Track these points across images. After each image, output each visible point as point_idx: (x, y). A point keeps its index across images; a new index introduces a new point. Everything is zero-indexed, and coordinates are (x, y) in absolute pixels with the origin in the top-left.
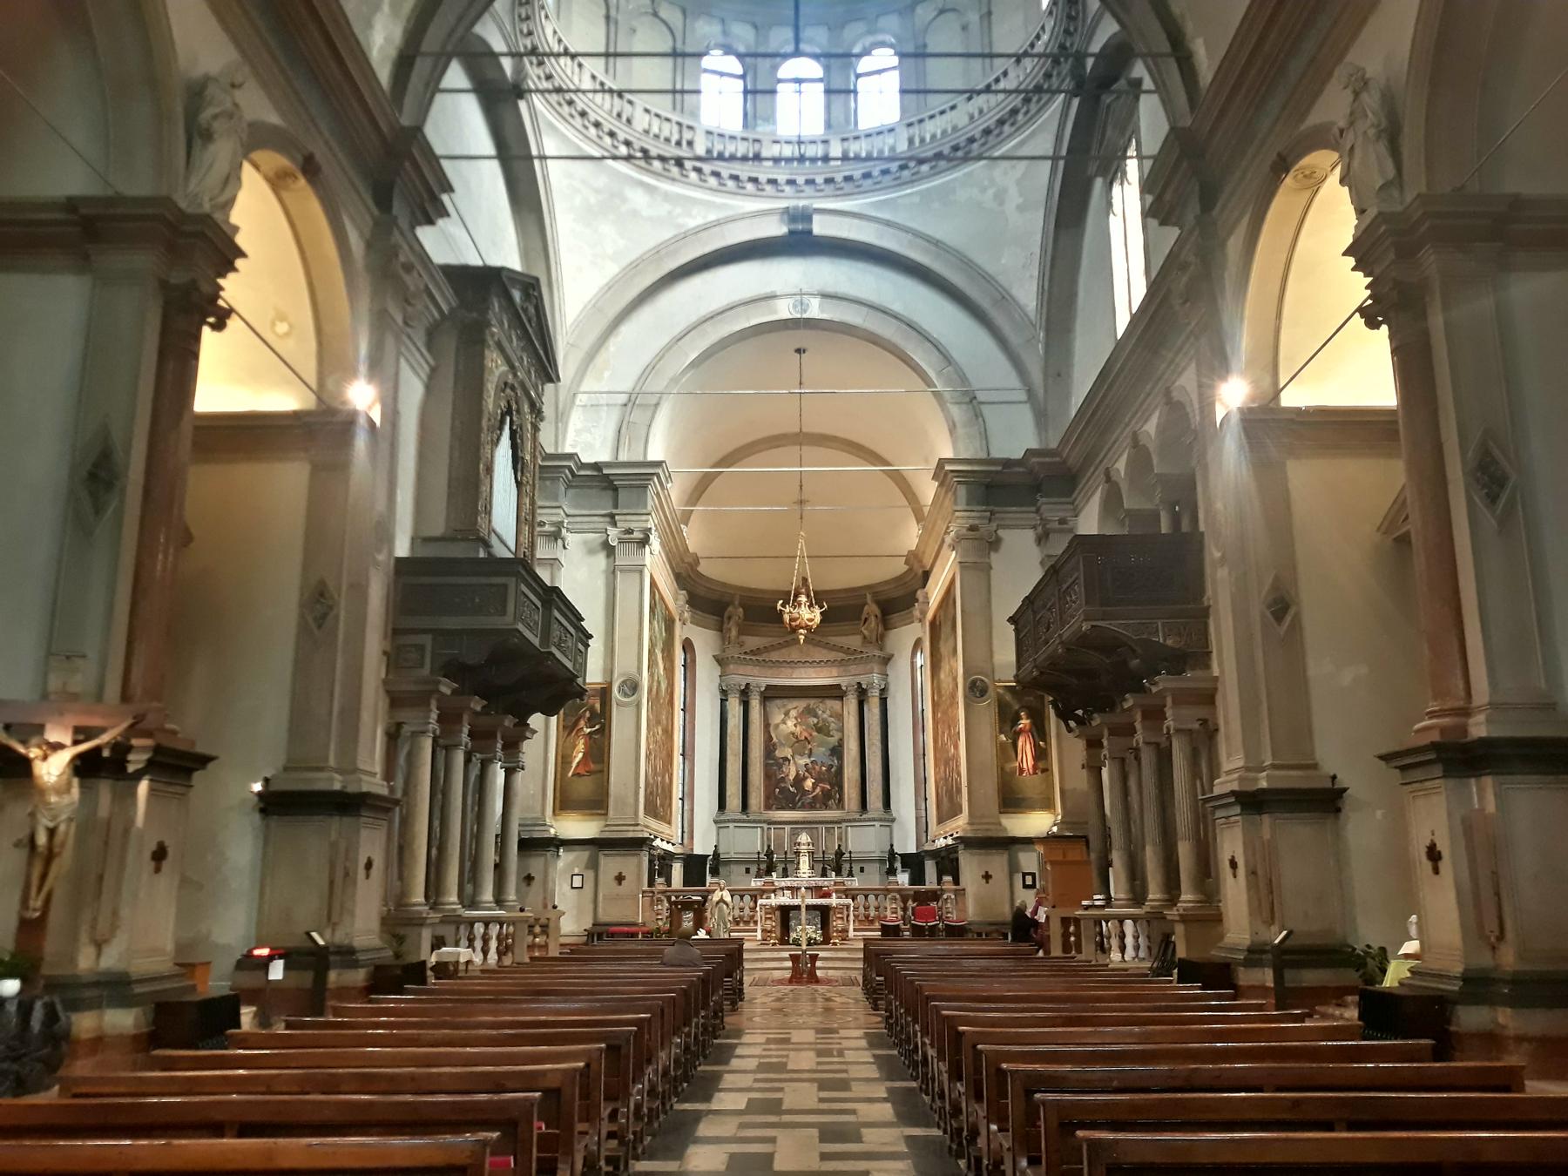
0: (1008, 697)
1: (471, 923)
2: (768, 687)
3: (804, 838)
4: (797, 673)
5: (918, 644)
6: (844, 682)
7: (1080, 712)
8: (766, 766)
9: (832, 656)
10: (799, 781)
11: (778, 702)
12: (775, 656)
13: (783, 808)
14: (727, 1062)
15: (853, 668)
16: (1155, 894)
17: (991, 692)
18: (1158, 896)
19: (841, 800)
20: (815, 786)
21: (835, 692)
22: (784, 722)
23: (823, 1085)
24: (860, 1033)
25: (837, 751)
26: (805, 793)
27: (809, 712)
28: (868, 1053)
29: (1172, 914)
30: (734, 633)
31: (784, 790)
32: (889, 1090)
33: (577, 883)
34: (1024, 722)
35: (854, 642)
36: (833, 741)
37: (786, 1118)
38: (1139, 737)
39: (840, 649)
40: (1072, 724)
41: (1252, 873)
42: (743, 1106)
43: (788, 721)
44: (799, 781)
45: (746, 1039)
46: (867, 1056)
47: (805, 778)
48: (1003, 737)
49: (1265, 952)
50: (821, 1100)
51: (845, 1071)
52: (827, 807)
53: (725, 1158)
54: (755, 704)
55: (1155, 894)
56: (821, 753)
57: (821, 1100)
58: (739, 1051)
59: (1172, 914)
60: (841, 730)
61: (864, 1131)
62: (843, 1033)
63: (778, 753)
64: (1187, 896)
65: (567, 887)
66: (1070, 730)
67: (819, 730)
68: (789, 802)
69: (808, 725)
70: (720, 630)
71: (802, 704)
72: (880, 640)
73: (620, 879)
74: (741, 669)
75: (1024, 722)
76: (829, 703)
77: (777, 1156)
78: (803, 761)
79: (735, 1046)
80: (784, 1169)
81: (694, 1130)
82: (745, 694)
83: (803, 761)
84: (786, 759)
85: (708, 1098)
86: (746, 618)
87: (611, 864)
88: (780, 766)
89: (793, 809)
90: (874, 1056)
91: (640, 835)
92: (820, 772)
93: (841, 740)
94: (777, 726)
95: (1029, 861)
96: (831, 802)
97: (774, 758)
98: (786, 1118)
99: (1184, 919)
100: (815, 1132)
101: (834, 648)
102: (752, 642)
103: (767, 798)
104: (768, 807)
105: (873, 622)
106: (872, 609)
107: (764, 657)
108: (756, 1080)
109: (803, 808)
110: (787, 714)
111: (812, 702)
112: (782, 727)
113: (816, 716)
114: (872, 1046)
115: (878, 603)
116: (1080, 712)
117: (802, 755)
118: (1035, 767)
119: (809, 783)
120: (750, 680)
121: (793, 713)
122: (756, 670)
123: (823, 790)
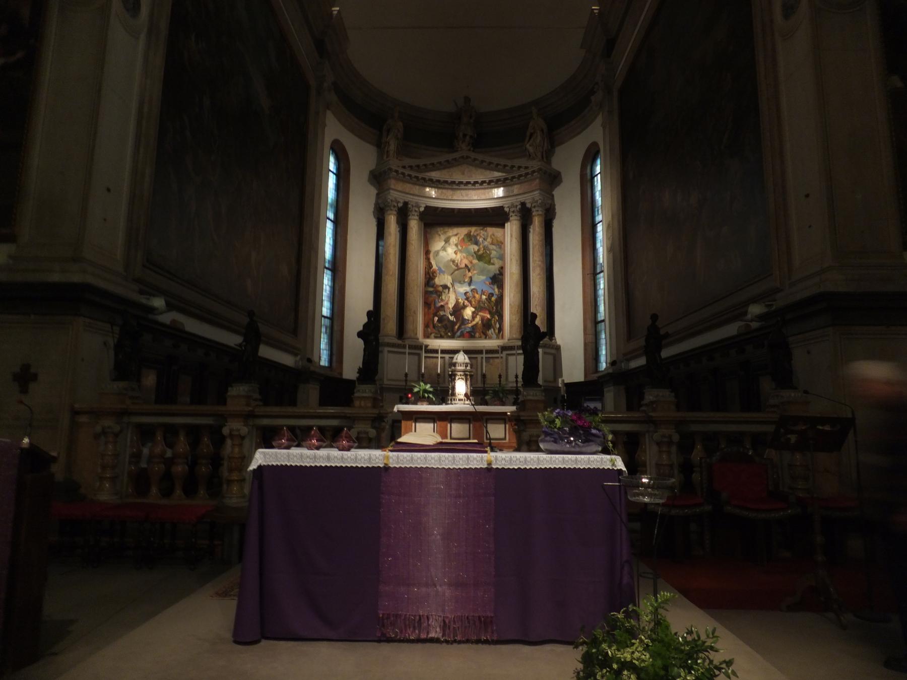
2: (427, 207)
3: (461, 358)
4: (458, 194)
8: (427, 294)
9: (497, 174)
10: (458, 310)
11: (440, 230)
12: (435, 175)
13: (441, 337)
19: (501, 329)
20: (474, 315)
22: (444, 249)
25: (497, 280)
26: (464, 321)
30: (392, 147)
36: (493, 269)
43: (449, 249)
44: (458, 310)
47: (464, 307)
52: (486, 336)
54: (414, 225)
56: (481, 280)
60: (502, 257)
63: (439, 281)
67: (480, 258)
68: (448, 329)
69: (468, 252)
71: (463, 231)
74: (400, 186)
76: (491, 230)
78: (463, 289)
82: (403, 215)
83: (463, 289)
84: (445, 287)
88: (439, 294)
89: (452, 337)
91: (76, 278)
92: (480, 301)
93: (502, 268)
94: (437, 253)
96: (491, 332)
97: (433, 286)
103: (426, 326)
104: (427, 336)
109: (462, 336)
110: (447, 241)
111: (473, 230)
112: (442, 254)
113: (476, 243)
117: (461, 282)
119: (468, 312)
120: (408, 198)
121: (454, 240)
123: (482, 319)
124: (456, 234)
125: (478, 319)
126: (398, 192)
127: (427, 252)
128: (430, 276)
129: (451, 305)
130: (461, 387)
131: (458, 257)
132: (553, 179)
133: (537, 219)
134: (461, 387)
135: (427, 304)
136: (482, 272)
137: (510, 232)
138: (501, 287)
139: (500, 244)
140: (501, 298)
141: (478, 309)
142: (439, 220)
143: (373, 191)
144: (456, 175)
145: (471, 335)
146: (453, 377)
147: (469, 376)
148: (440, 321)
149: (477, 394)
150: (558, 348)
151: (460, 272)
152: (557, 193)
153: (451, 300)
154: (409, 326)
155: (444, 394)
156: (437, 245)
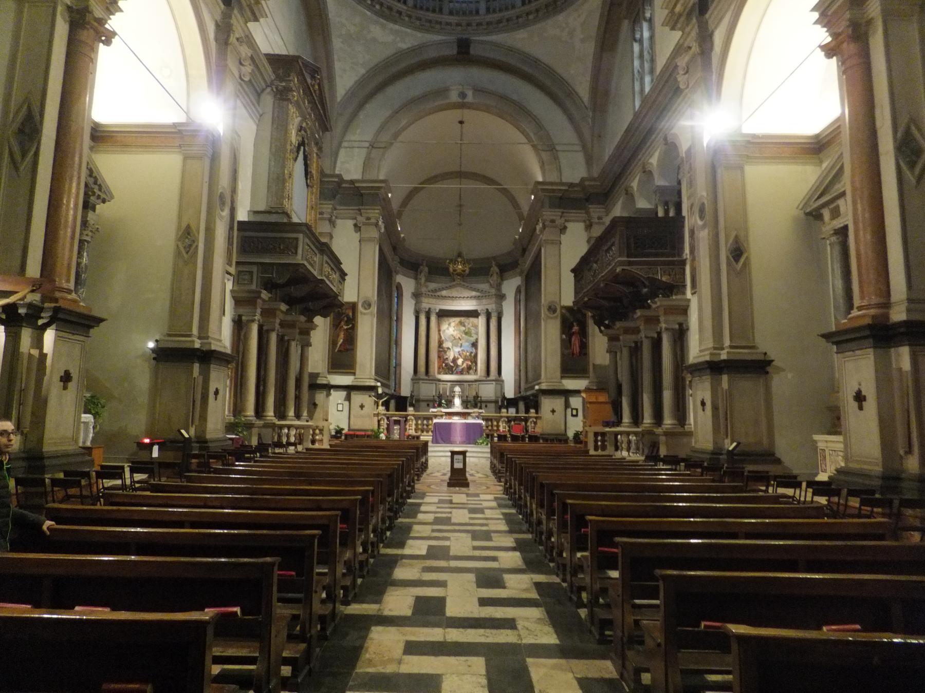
0: (568, 314)
1: (281, 427)
2: (441, 310)
4: (455, 302)
5: (518, 291)
6: (479, 308)
7: (607, 322)
8: (439, 351)
9: (474, 293)
10: (455, 360)
11: (446, 319)
12: (444, 293)
14: (415, 516)
15: (484, 301)
16: (648, 420)
17: (558, 311)
18: (649, 421)
19: (476, 370)
21: (474, 314)
23: (475, 536)
24: (491, 497)
25: (475, 345)
27: (461, 323)
28: (498, 511)
29: (659, 431)
30: (423, 280)
31: (446, 365)
32: (517, 541)
33: (340, 408)
34: (576, 328)
35: (484, 286)
36: (473, 339)
37: (454, 564)
38: (642, 334)
39: (478, 291)
40: (602, 328)
41: (715, 408)
42: (424, 552)
43: (450, 329)
44: (455, 360)
45: (427, 499)
46: (497, 514)
48: (564, 336)
49: (721, 454)
50: (475, 548)
51: (486, 525)
52: (468, 373)
53: (410, 601)
54: (433, 319)
55: (648, 420)
56: (467, 346)
57: (475, 548)
58: (423, 508)
59: (659, 431)
60: (477, 334)
61: (506, 577)
62: (482, 497)
63: (445, 345)
64: (668, 421)
65: (335, 411)
66: (601, 331)
67: (466, 333)
68: (450, 370)
70: (416, 279)
71: (457, 320)
72: (499, 287)
73: (362, 407)
75: (576, 328)
76: (472, 320)
77: (448, 601)
78: (457, 349)
79: (419, 505)
80: (453, 615)
81: (390, 574)
83: (457, 349)
84: (448, 348)
85: (402, 545)
86: (430, 273)
87: (358, 398)
88: (445, 352)
89: (452, 374)
90: (504, 514)
95: (576, 402)
96: (471, 371)
98: (454, 564)
99: (666, 434)
100: (472, 577)
101: (474, 290)
102: (432, 286)
103: (439, 368)
104: (439, 373)
105: (495, 277)
106: (495, 269)
107: (439, 293)
108: (433, 531)
109: (457, 373)
110: (449, 324)
111: (463, 319)
112: (447, 331)
113: (464, 326)
114: (500, 506)
115: (499, 266)
116: (607, 322)
118: (580, 353)
119: (460, 362)
121: (453, 324)
122: (434, 301)
124: (455, 321)
125: (465, 365)
126: (426, 304)
127: (439, 331)
128: (440, 343)
129: (451, 358)
130: (457, 401)
131: (455, 333)
132: (501, 297)
133: (494, 318)
134: (457, 401)
135: (439, 357)
136: (467, 341)
137: (481, 321)
138: (476, 348)
139: (476, 327)
140: (476, 356)
141: (465, 359)
142: (444, 314)
143: (413, 302)
144: (454, 293)
145: (461, 373)
146: (454, 397)
147: (461, 397)
148: (446, 365)
149: (465, 403)
150: (503, 381)
151: (456, 341)
152: (504, 303)
153: (451, 355)
154: (431, 370)
155: (450, 403)
156: (444, 327)
